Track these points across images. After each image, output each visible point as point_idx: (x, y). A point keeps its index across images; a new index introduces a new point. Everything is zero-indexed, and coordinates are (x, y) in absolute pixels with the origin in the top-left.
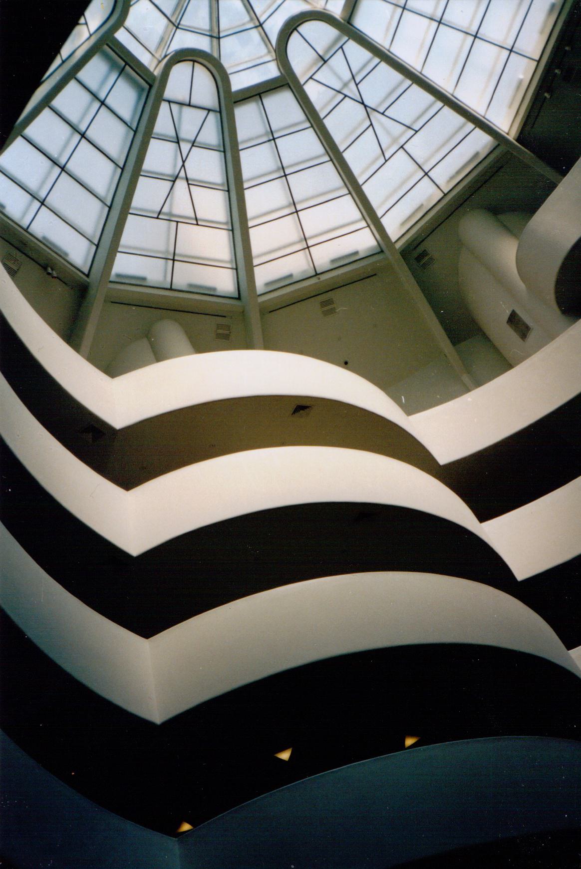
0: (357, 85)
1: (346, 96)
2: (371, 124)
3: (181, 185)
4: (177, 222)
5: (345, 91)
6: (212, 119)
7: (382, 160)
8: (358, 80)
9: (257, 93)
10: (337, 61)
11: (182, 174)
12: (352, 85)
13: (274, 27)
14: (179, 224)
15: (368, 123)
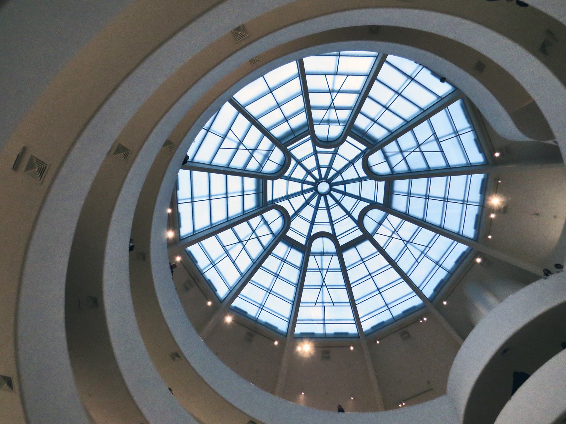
0: (397, 232)
1: (393, 238)
2: (408, 248)
3: (325, 288)
4: (325, 306)
5: (394, 236)
6: (336, 258)
7: (417, 263)
8: (397, 231)
9: (353, 244)
10: (386, 222)
11: (324, 284)
12: (396, 232)
13: (356, 215)
14: (325, 307)
15: (406, 248)
